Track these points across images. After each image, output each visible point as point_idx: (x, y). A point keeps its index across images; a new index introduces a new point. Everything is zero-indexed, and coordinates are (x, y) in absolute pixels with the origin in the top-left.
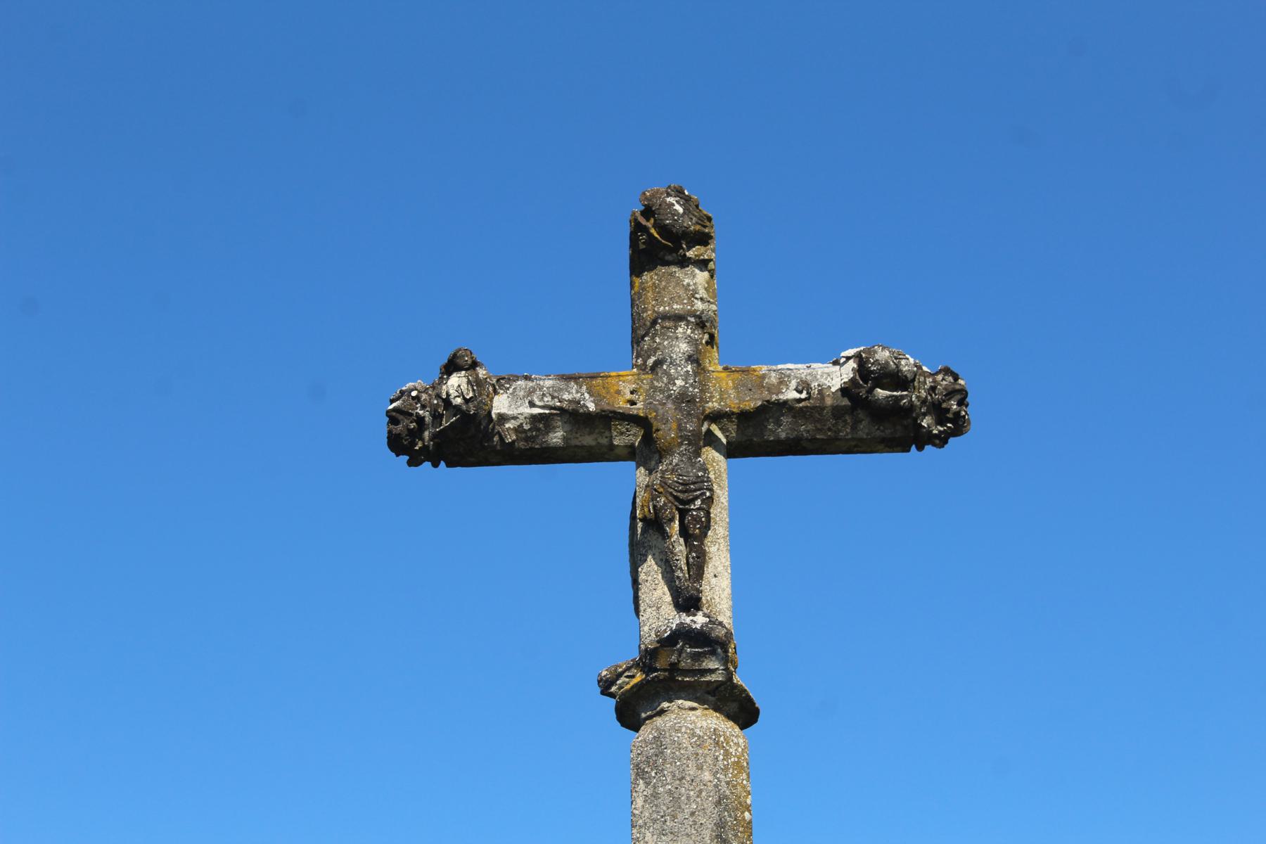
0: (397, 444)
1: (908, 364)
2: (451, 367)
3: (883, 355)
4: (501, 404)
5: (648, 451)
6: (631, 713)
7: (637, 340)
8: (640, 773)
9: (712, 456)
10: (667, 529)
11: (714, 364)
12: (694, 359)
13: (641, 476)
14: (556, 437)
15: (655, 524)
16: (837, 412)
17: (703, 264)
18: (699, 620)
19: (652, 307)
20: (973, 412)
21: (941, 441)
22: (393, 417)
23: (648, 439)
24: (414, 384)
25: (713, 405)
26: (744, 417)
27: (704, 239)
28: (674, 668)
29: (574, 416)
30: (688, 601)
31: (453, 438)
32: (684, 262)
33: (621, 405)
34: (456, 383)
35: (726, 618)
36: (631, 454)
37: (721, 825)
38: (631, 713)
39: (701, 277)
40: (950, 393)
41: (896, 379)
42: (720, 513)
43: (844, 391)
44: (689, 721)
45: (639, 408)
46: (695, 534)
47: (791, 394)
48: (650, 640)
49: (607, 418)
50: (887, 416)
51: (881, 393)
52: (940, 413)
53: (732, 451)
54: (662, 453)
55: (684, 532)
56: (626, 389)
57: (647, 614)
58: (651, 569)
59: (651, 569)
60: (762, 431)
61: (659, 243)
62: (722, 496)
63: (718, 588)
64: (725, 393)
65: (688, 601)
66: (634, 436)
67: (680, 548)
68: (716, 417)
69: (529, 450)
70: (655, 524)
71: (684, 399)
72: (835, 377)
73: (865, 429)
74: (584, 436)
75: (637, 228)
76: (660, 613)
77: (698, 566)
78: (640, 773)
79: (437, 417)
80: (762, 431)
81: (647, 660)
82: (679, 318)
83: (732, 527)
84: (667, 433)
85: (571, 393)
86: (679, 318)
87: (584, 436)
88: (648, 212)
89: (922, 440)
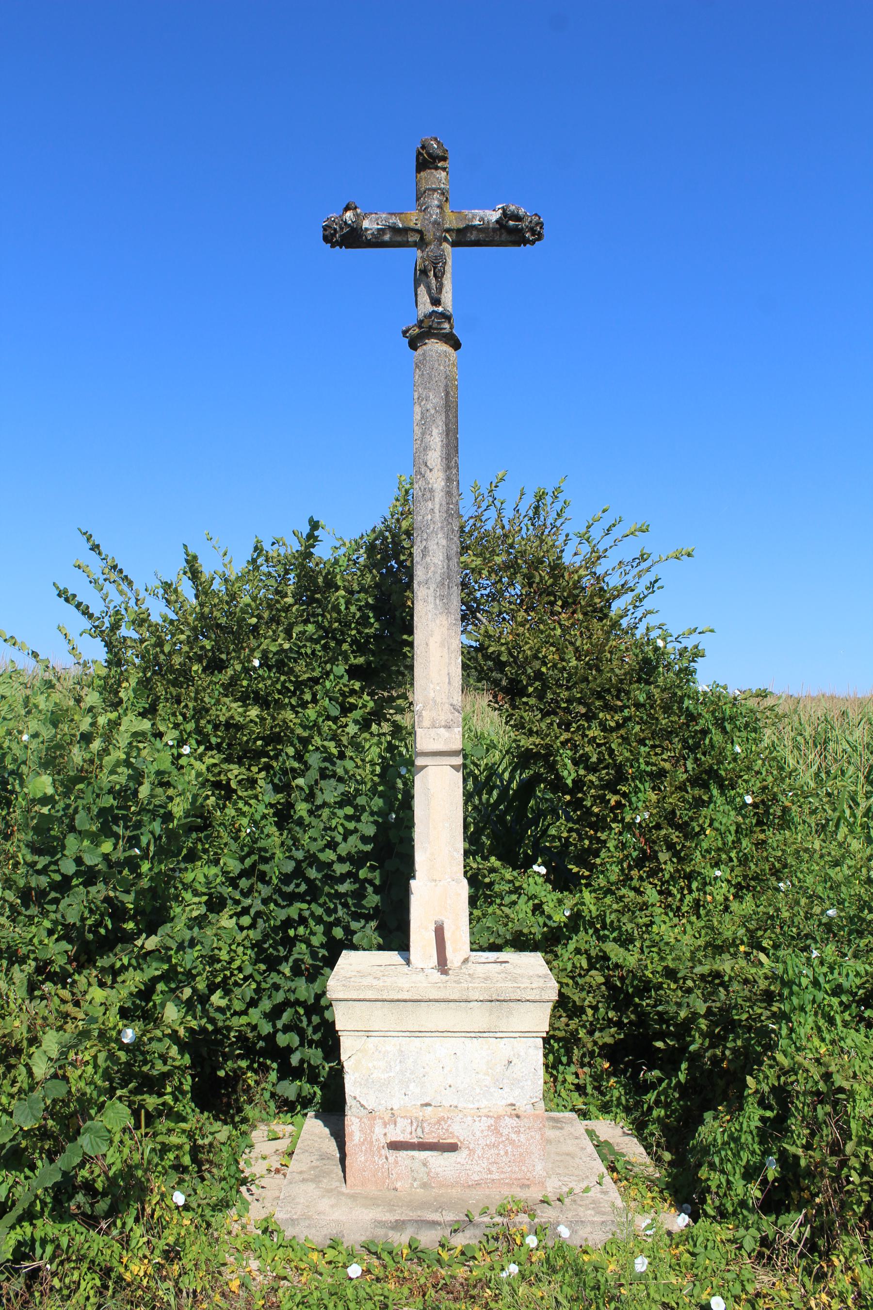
0: (326, 239)
1: (522, 211)
2: (347, 209)
3: (512, 208)
4: (366, 224)
5: (422, 244)
6: (414, 344)
7: (418, 199)
8: (417, 366)
9: (446, 246)
10: (428, 274)
11: (447, 209)
12: (440, 207)
13: (419, 253)
14: (387, 237)
15: (424, 272)
16: (494, 230)
17: (444, 169)
18: (440, 309)
19: (424, 186)
20: (545, 232)
21: (533, 243)
22: (325, 228)
23: (422, 239)
24: (333, 215)
25: (447, 226)
26: (459, 231)
27: (444, 159)
28: (430, 327)
29: (394, 229)
30: (436, 302)
31: (350, 238)
32: (437, 168)
33: (412, 225)
34: (349, 215)
35: (450, 309)
36: (415, 244)
37: (446, 386)
38: (414, 344)
39: (444, 174)
40: (537, 224)
41: (517, 218)
42: (449, 268)
43: (497, 222)
44: (435, 347)
45: (419, 227)
46: (439, 277)
47: (477, 223)
48: (421, 317)
49: (406, 230)
50: (512, 232)
51: (511, 223)
52: (533, 231)
53: (454, 244)
54: (427, 244)
55: (435, 275)
56: (414, 219)
57: (420, 306)
58: (422, 290)
59: (422, 290)
60: (464, 237)
61: (427, 161)
62: (449, 262)
63: (447, 297)
64: (452, 221)
65: (436, 302)
66: (416, 238)
67: (433, 281)
68: (448, 231)
69: (376, 243)
70: (424, 272)
71: (436, 223)
72: (494, 216)
73: (504, 237)
74: (398, 237)
75: (419, 154)
76: (425, 306)
77: (440, 289)
78: (417, 366)
79: (341, 229)
80: (464, 237)
81: (420, 324)
82: (435, 190)
83: (453, 274)
84: (429, 236)
85: (393, 220)
86: (435, 190)
87: (398, 237)
88: (423, 147)
89: (526, 242)
